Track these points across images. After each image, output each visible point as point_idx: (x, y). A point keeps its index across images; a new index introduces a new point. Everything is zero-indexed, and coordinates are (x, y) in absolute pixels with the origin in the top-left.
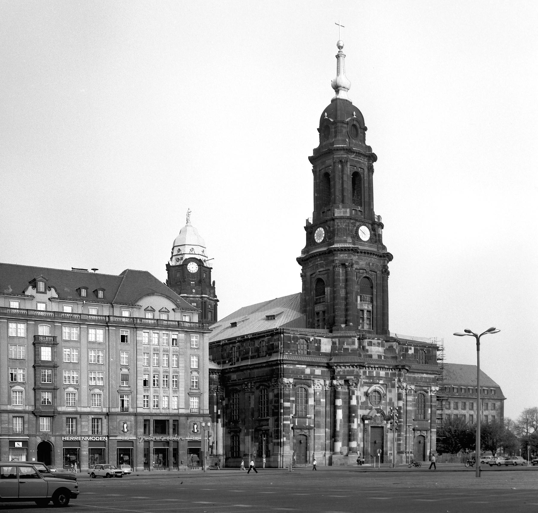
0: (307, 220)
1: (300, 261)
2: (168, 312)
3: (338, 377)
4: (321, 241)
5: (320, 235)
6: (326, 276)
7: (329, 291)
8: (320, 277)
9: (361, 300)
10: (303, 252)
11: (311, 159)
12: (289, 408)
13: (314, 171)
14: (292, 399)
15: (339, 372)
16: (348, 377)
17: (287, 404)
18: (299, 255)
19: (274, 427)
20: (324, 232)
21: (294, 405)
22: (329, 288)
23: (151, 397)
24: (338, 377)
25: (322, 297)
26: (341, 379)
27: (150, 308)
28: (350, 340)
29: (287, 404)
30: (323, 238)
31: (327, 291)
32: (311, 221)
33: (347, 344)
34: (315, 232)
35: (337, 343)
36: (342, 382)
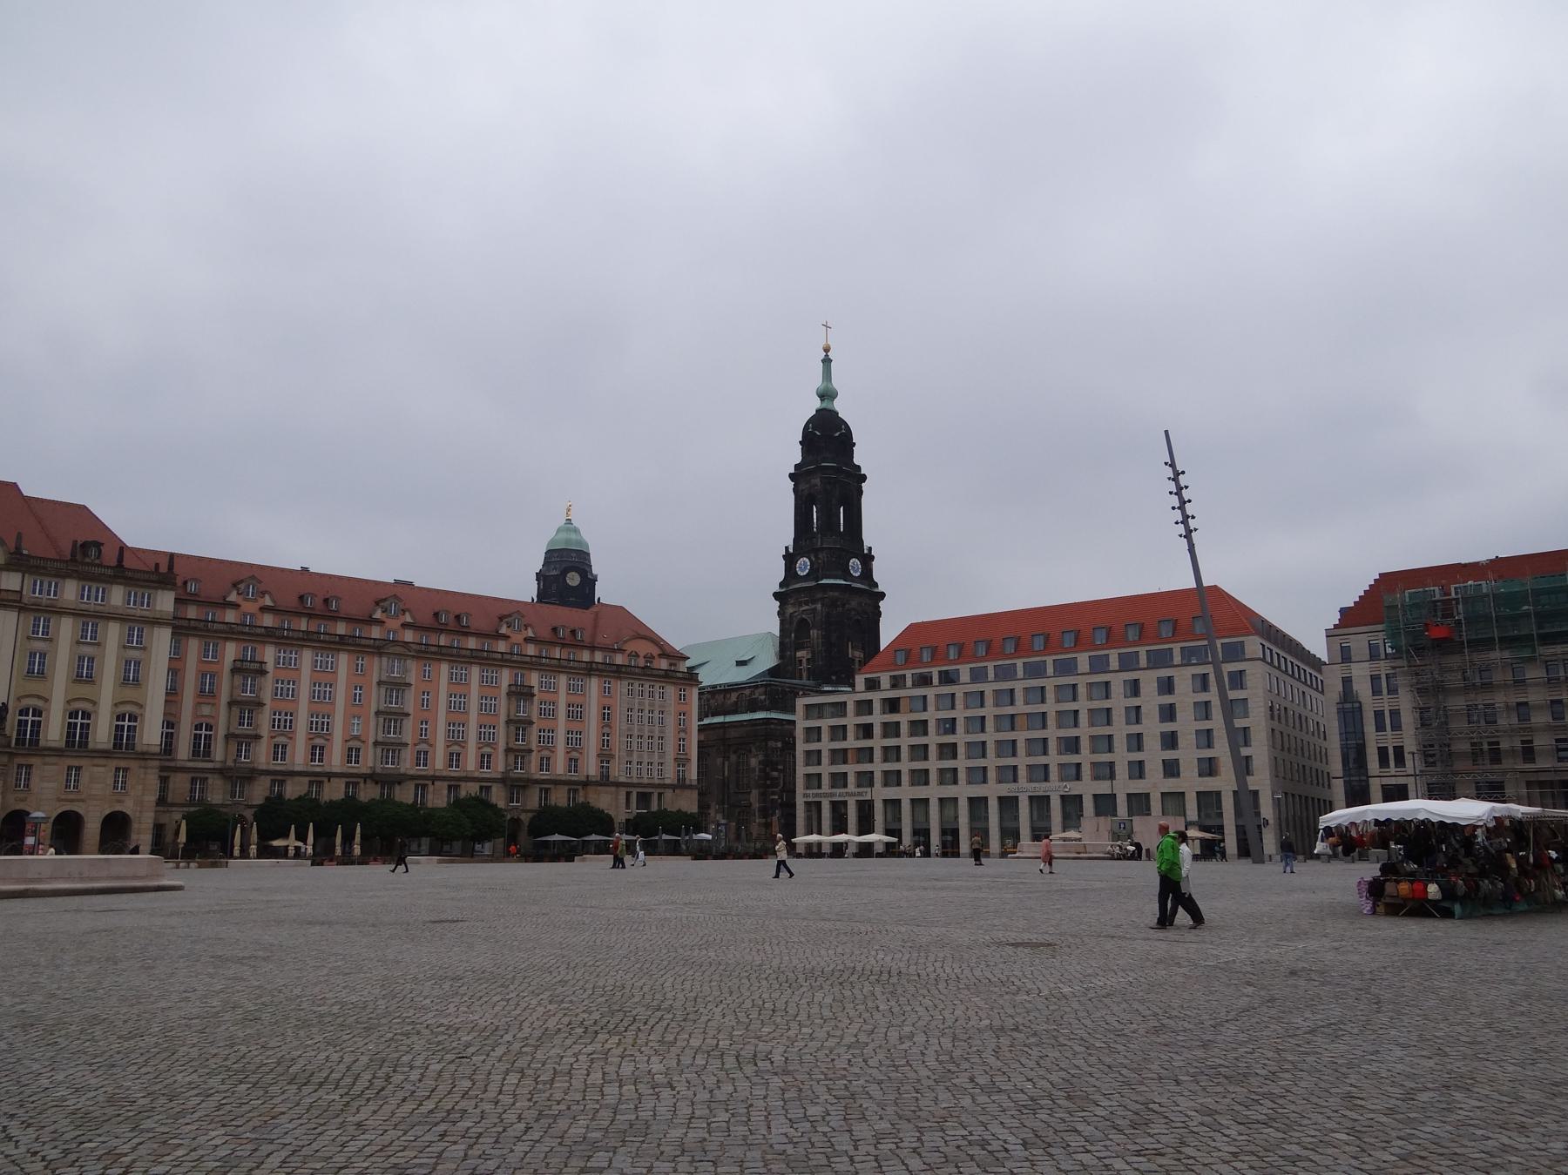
0: (787, 548)
1: (776, 596)
2: (654, 658)
4: (805, 573)
5: (803, 566)
9: (852, 647)
10: (781, 585)
11: (791, 476)
12: (777, 779)
13: (795, 490)
14: (780, 767)
17: (775, 774)
18: (777, 589)
19: (759, 803)
20: (809, 563)
21: (782, 775)
22: (815, 631)
23: (635, 762)
27: (634, 653)
29: (775, 774)
30: (807, 571)
32: (791, 550)
34: (796, 562)
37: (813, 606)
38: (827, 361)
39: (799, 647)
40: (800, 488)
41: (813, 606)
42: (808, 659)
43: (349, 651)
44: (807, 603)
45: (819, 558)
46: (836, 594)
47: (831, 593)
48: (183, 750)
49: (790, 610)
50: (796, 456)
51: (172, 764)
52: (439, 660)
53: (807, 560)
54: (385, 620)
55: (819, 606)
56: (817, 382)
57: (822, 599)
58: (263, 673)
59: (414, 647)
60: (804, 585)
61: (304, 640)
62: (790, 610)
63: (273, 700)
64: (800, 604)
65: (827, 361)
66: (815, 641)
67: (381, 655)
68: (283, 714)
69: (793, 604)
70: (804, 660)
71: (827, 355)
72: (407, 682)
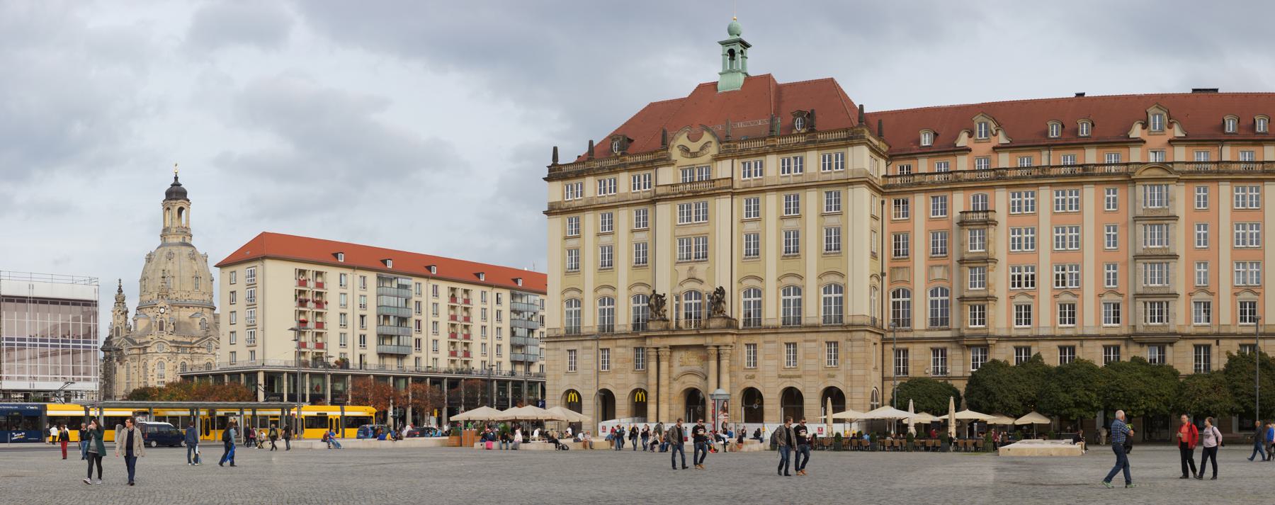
43: (1096, 183)
48: (920, 319)
51: (910, 335)
52: (1218, 180)
54: (1144, 138)
58: (989, 223)
59: (1177, 167)
61: (1037, 177)
63: (1009, 253)
67: (1134, 181)
68: (1023, 269)
72: (1171, 213)
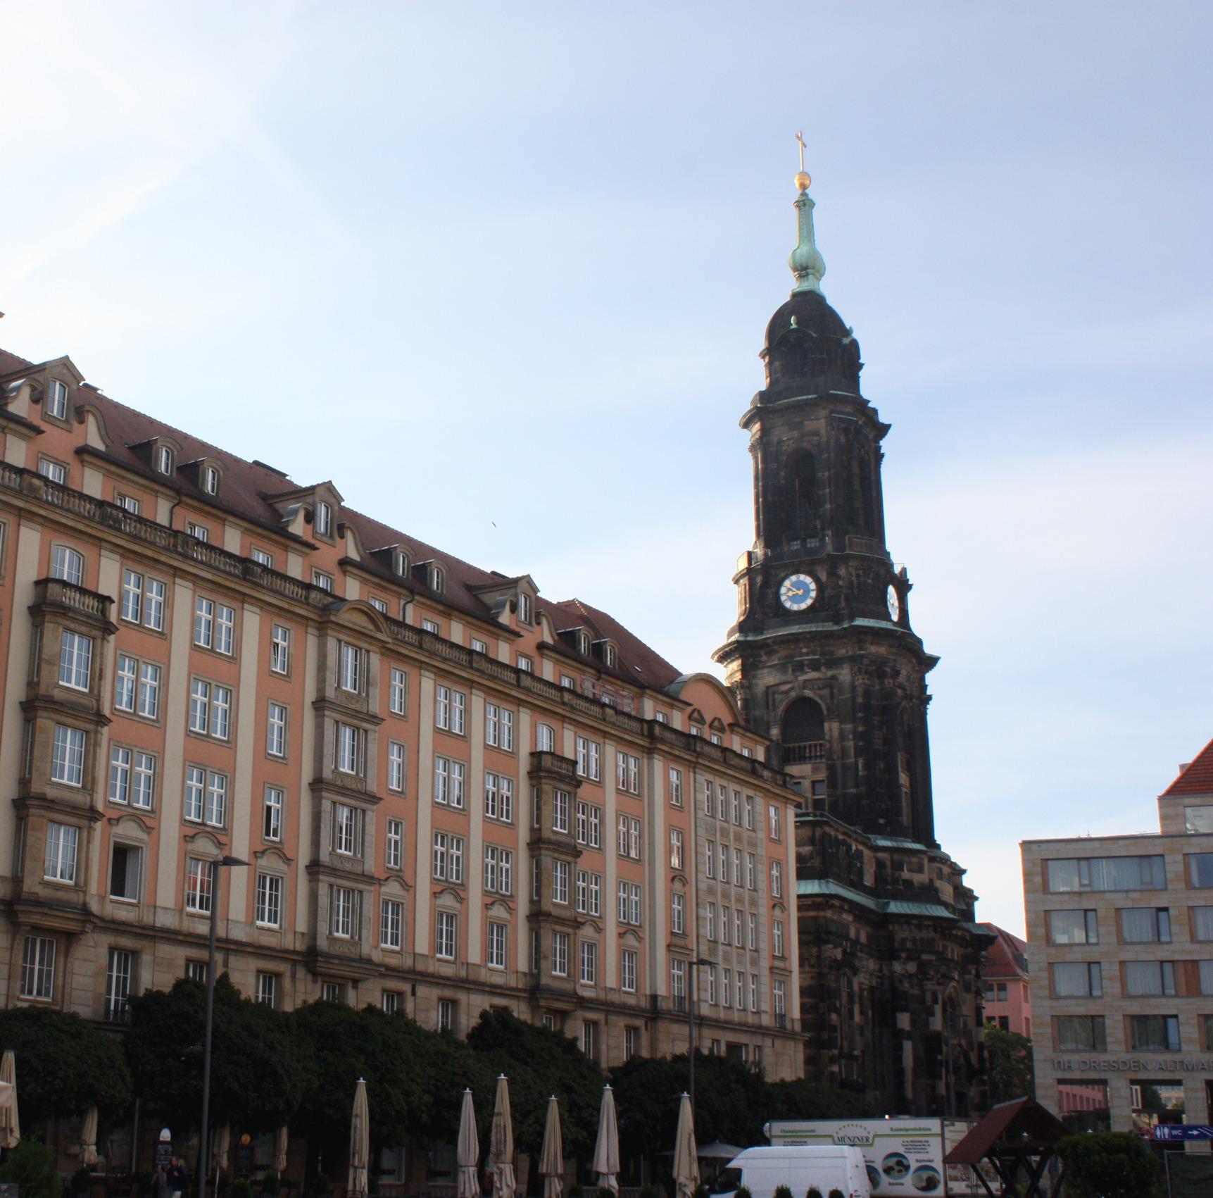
3: (904, 955)
6: (825, 692)
7: (836, 733)
8: (808, 693)
15: (904, 940)
16: (924, 957)
20: (813, 586)
22: (835, 725)
24: (904, 955)
25: (815, 746)
26: (909, 959)
28: (915, 860)
30: (809, 602)
31: (831, 730)
33: (911, 870)
35: (888, 864)
36: (912, 967)
37: (830, 673)
38: (804, 204)
39: (801, 758)
40: (776, 439)
41: (830, 673)
42: (814, 783)
44: (815, 666)
45: (839, 577)
46: (882, 650)
47: (873, 649)
49: (767, 678)
50: (757, 378)
53: (808, 580)
55: (844, 674)
56: (788, 242)
57: (852, 659)
60: (813, 628)
62: (767, 678)
64: (799, 667)
65: (804, 204)
66: (836, 747)
69: (782, 667)
70: (806, 784)
71: (804, 194)
